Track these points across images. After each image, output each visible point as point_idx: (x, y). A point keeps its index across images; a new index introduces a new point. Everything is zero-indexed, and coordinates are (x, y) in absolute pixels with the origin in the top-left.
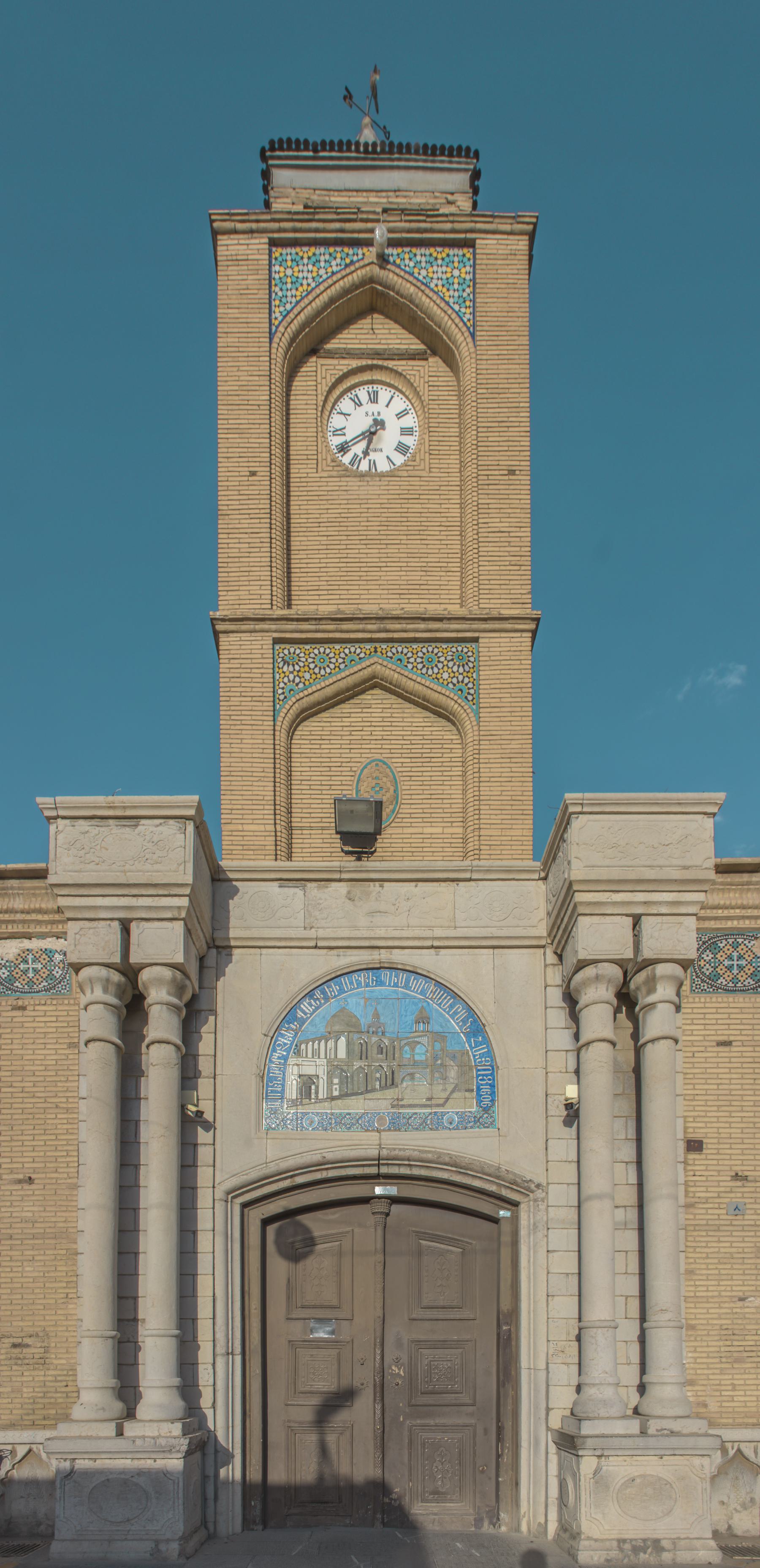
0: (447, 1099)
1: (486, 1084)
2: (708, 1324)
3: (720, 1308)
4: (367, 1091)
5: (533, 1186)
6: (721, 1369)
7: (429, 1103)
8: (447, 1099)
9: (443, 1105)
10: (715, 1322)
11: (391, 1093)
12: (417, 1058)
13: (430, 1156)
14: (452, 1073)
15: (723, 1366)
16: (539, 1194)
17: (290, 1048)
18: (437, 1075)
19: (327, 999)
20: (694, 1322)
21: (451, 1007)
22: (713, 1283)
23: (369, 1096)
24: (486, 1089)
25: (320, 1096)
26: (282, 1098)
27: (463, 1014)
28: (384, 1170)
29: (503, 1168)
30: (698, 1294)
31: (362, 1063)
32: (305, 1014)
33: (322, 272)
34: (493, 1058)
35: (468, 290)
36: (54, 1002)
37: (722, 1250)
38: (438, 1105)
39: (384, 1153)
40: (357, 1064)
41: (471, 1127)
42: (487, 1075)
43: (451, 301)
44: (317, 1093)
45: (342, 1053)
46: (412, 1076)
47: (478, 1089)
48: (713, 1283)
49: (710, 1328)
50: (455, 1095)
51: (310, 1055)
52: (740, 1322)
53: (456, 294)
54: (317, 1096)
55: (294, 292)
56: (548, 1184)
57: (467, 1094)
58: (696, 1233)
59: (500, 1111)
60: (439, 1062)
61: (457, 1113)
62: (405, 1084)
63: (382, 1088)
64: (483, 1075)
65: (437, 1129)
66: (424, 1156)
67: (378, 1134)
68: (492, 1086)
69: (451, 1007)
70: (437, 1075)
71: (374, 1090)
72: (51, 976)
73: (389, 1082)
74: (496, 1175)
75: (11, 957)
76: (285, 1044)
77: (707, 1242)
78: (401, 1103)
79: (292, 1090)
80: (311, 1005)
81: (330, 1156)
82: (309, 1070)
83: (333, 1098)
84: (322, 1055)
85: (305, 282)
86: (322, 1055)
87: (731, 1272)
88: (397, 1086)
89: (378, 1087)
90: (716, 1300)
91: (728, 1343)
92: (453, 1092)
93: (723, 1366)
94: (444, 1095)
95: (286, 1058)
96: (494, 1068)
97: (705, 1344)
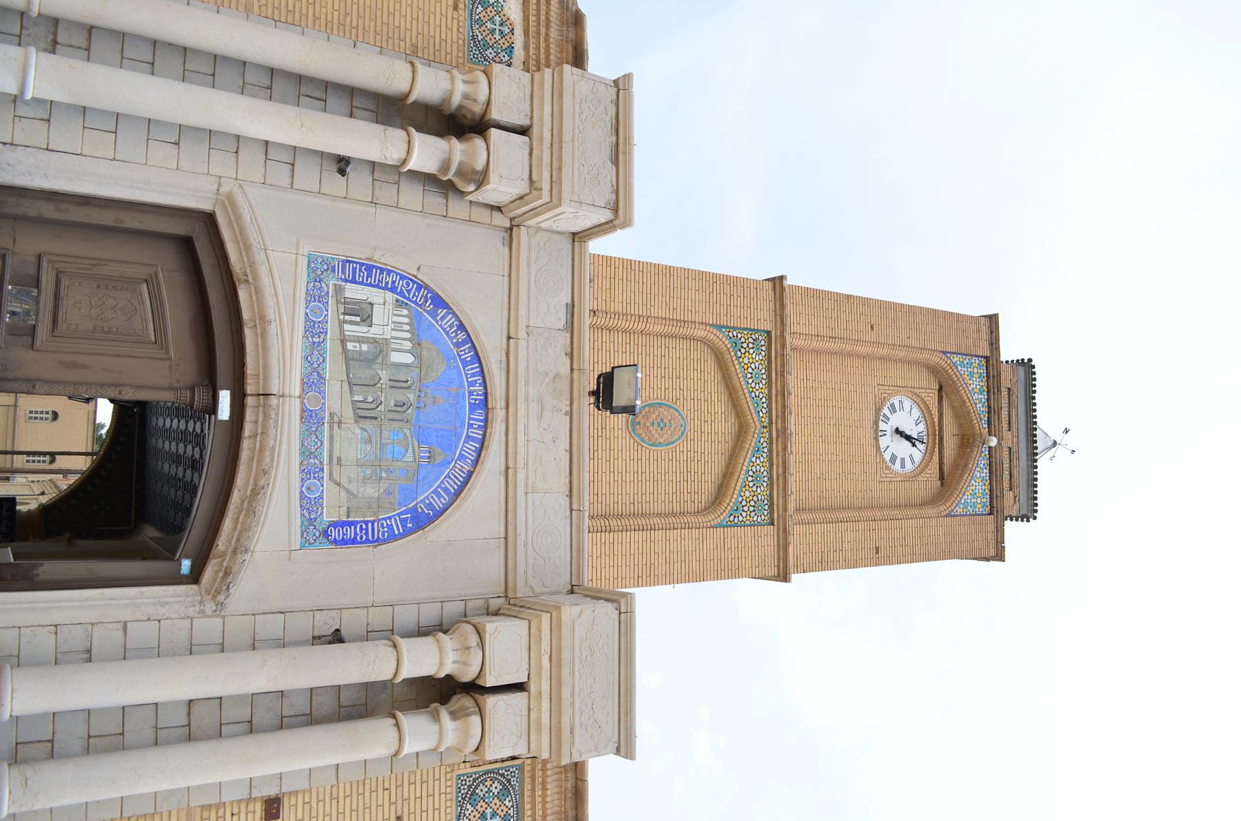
1: (356, 534)
5: (221, 598)
7: (335, 461)
8: (338, 484)
9: (331, 478)
11: (349, 414)
12: (389, 448)
13: (267, 460)
14: (370, 491)
16: (210, 607)
17: (404, 297)
18: (368, 471)
19: (457, 345)
21: (446, 490)
23: (346, 385)
24: (350, 532)
25: (347, 327)
26: (346, 281)
27: (438, 504)
28: (250, 401)
29: (247, 557)
32: (442, 319)
34: (386, 541)
36: (461, 42)
38: (331, 473)
39: (273, 401)
41: (303, 515)
42: (367, 534)
44: (352, 323)
45: (396, 357)
46: (368, 441)
47: (351, 524)
50: (343, 493)
54: (345, 322)
56: (223, 617)
57: (345, 509)
59: (327, 552)
60: (384, 475)
62: (358, 431)
64: (367, 529)
66: (268, 453)
67: (297, 394)
68: (353, 541)
69: (446, 490)
70: (368, 471)
72: (487, 46)
73: (362, 413)
74: (239, 548)
75: (506, 9)
76: (409, 292)
78: (336, 426)
79: (354, 292)
80: (451, 326)
81: (273, 329)
82: (378, 315)
83: (343, 342)
88: (356, 422)
89: (356, 398)
92: (347, 490)
94: (344, 481)
95: (393, 290)
96: (377, 542)
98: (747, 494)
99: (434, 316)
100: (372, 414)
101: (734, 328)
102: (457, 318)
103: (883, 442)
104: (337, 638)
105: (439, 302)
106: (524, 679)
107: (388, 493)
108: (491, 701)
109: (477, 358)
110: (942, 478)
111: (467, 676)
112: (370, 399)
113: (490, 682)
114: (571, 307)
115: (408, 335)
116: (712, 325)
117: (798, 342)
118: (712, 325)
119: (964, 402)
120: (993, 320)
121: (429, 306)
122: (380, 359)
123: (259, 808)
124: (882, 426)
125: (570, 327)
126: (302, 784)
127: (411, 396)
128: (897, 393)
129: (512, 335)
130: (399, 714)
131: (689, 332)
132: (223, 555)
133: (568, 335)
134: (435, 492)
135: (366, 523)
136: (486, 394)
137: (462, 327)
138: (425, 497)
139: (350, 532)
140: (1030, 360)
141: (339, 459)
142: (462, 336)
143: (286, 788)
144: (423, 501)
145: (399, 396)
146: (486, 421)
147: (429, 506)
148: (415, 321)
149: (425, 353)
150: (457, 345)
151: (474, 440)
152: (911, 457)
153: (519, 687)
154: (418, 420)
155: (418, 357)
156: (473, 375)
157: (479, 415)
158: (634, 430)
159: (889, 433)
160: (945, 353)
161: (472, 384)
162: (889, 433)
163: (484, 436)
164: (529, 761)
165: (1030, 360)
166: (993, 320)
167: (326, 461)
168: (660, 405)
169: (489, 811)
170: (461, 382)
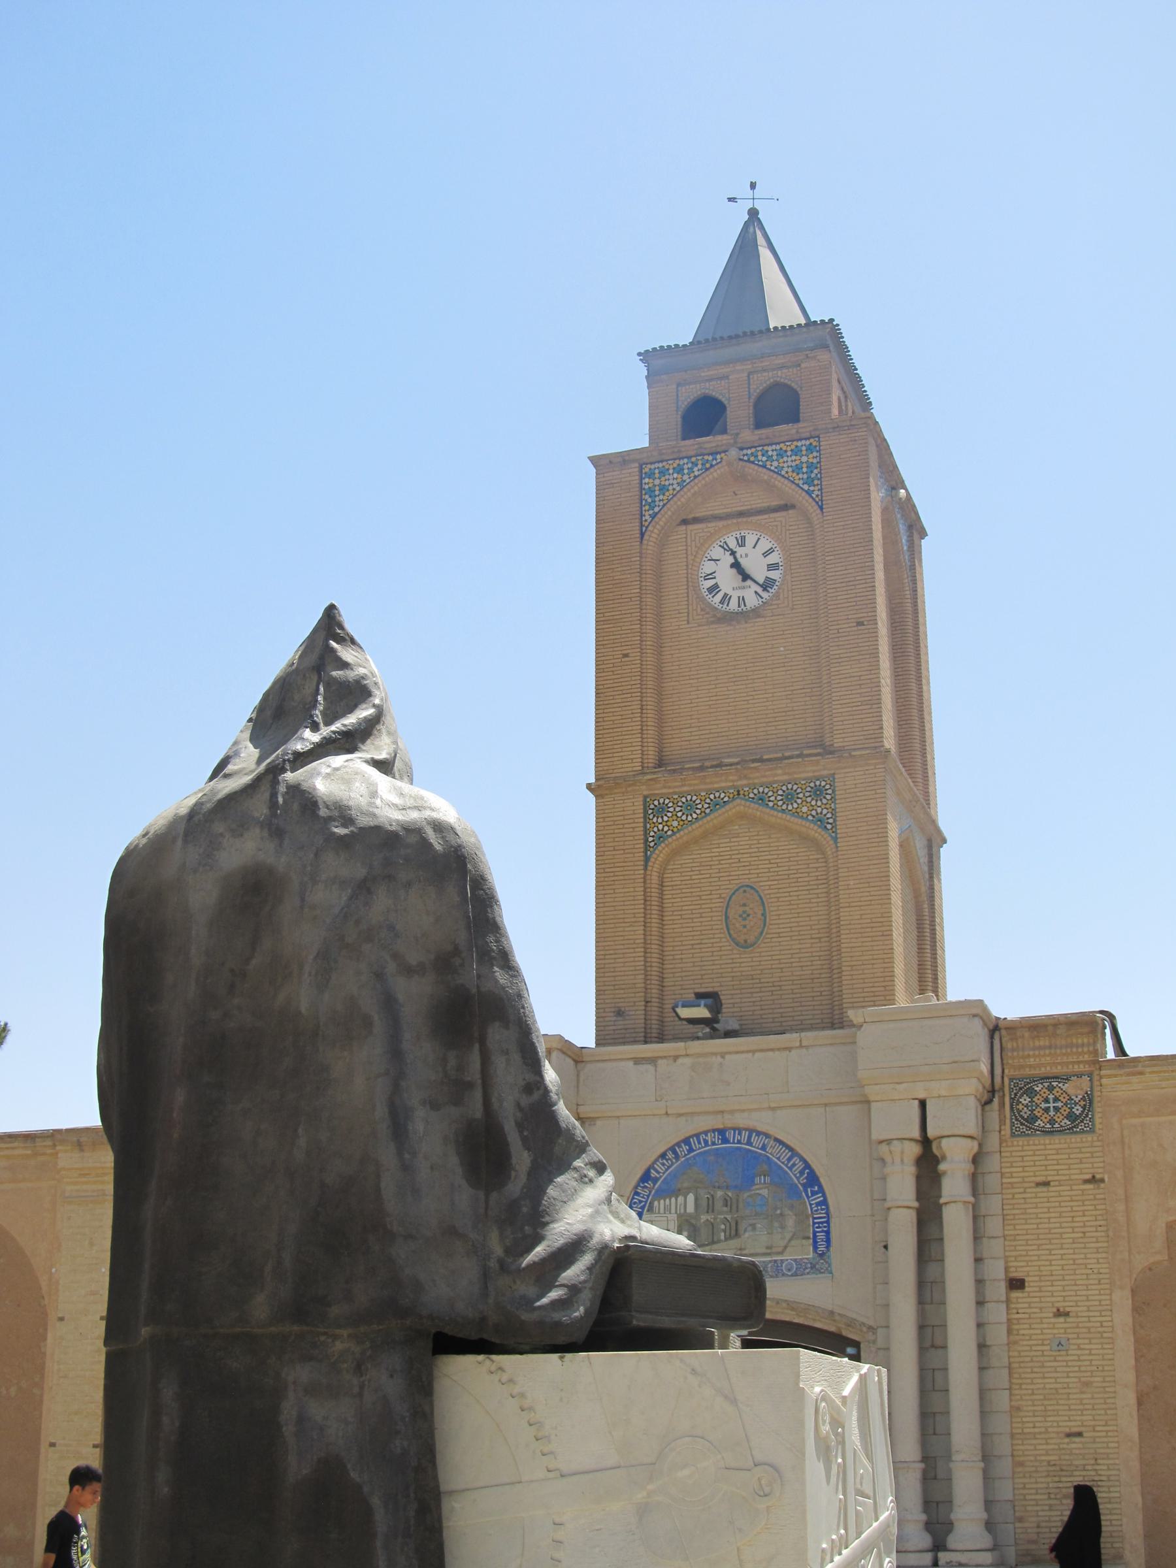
0: (786, 1247)
2: (1036, 1460)
3: (1047, 1444)
4: (713, 1242)
6: (1050, 1505)
8: (786, 1247)
9: (781, 1253)
10: (1043, 1458)
11: (734, 1243)
14: (790, 1222)
15: (1052, 1502)
18: (776, 1224)
20: (1022, 1459)
21: (789, 1159)
22: (1040, 1419)
24: (821, 1236)
27: (800, 1165)
30: (1026, 1431)
31: (710, 1217)
32: (658, 1172)
33: (686, 477)
34: (828, 1208)
35: (816, 471)
37: (1047, 1386)
40: (704, 1218)
43: (801, 482)
45: (691, 1209)
47: (815, 1236)
48: (1040, 1419)
49: (1037, 1464)
50: (793, 1243)
51: (662, 1210)
52: (1067, 1457)
53: (805, 476)
55: (661, 497)
58: (1021, 1370)
61: (795, 1260)
62: (747, 1235)
63: (726, 1239)
65: (777, 1276)
68: (828, 1233)
69: (789, 1159)
70: (776, 1224)
71: (719, 1241)
73: (733, 1233)
76: (640, 1202)
77: (1032, 1379)
80: (663, 1164)
84: (673, 1211)
85: (671, 488)
86: (673, 1211)
87: (1057, 1407)
90: (1043, 1436)
91: (1057, 1479)
92: (790, 1240)
93: (1052, 1502)
94: (783, 1243)
96: (828, 1213)
97: (1033, 1480)
98: (805, 809)
99: (655, 1180)
100: (733, 1224)
101: (646, 840)
102: (657, 1160)
103: (752, 601)
104: (886, 1247)
105: (646, 1177)
106: (916, 1102)
107: (792, 1207)
108: (931, 1133)
109: (686, 1141)
110: (785, 507)
111: (915, 1150)
112: (723, 1227)
113: (916, 1134)
114: (638, 1061)
115: (673, 1199)
116: (645, 869)
117: (652, 755)
118: (645, 869)
119: (694, 494)
120: (595, 460)
121: (649, 1184)
122: (693, 1221)
123: (1015, 1294)
124: (733, 605)
125: (653, 1061)
126: (1001, 1264)
127: (719, 1193)
128: (697, 588)
129: (664, 1112)
130: (942, 1201)
131: (655, 892)
132: (839, 1328)
133: (660, 1062)
134: (791, 1169)
135: (814, 1223)
136: (714, 1131)
137: (663, 1156)
138: (795, 1177)
139: (821, 1236)
140: (639, 354)
141: (767, 1248)
142: (670, 1155)
143: (1002, 1276)
144: (798, 1179)
145: (719, 1205)
146: (734, 1129)
147: (802, 1173)
148: (662, 1194)
149: (686, 1185)
150: (677, 1157)
151: (750, 1137)
152: (766, 554)
153: (923, 1104)
154: (736, 1187)
155: (689, 1190)
156: (699, 1143)
157: (730, 1135)
158: (752, 945)
159: (740, 593)
160: (642, 535)
161: (706, 1142)
162: (740, 593)
163: (746, 1129)
164: (1006, 1071)
165: (639, 354)
166: (595, 460)
167: (769, 1259)
168: (727, 918)
169: (1043, 1105)
170: (705, 1152)
